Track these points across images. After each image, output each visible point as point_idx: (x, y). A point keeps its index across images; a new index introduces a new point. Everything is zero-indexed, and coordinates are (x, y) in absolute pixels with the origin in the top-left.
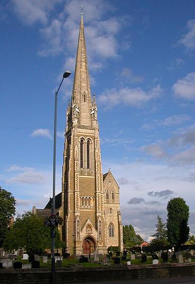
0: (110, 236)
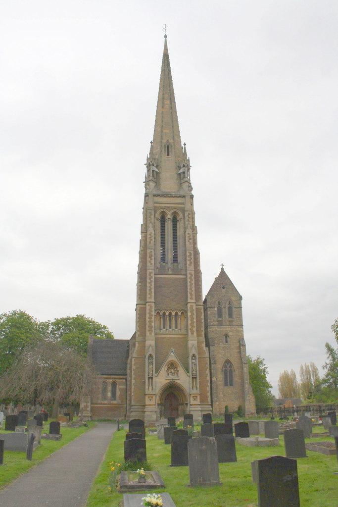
0: (226, 385)
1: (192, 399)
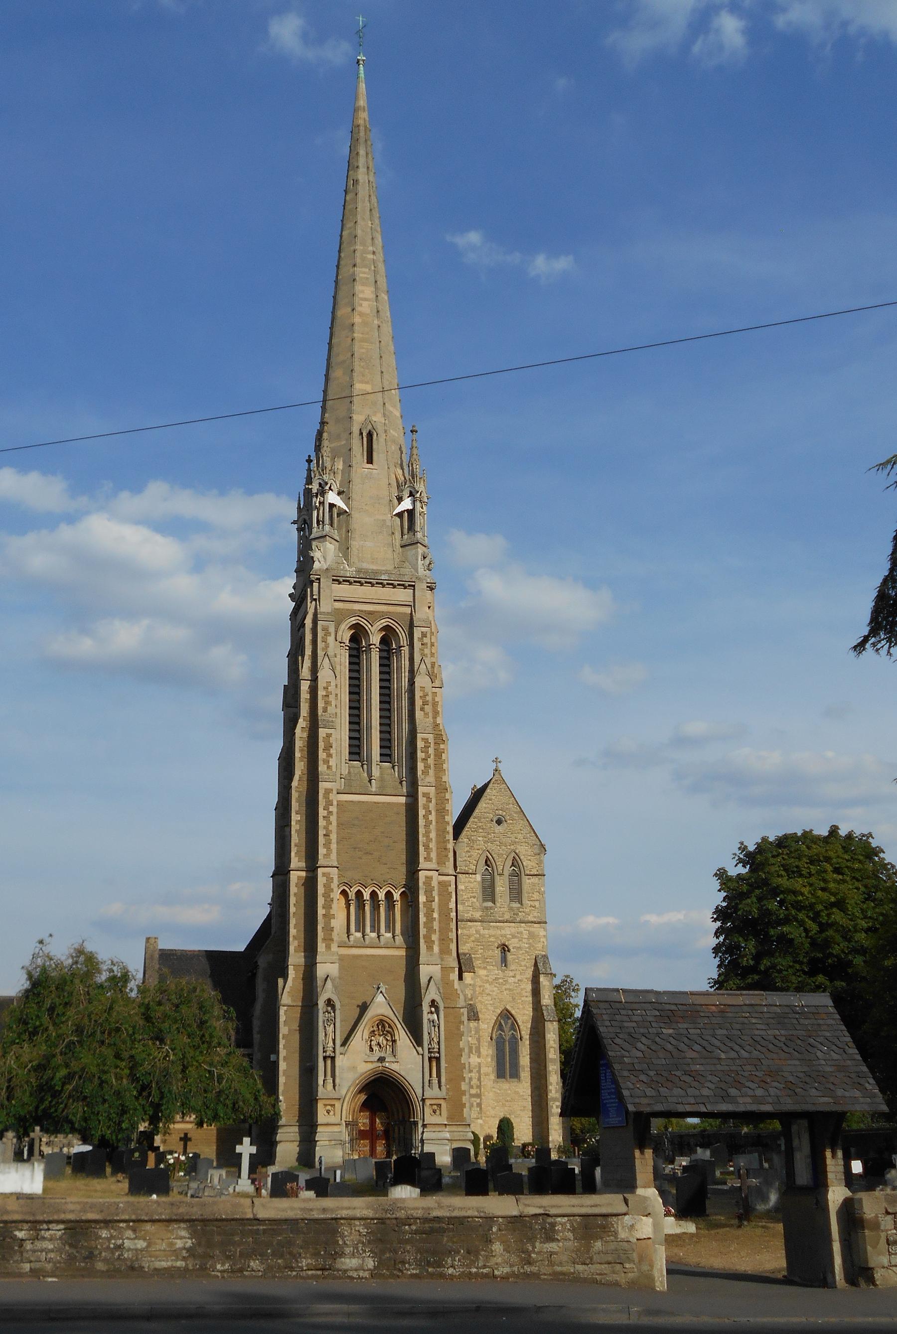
1: (428, 1110)
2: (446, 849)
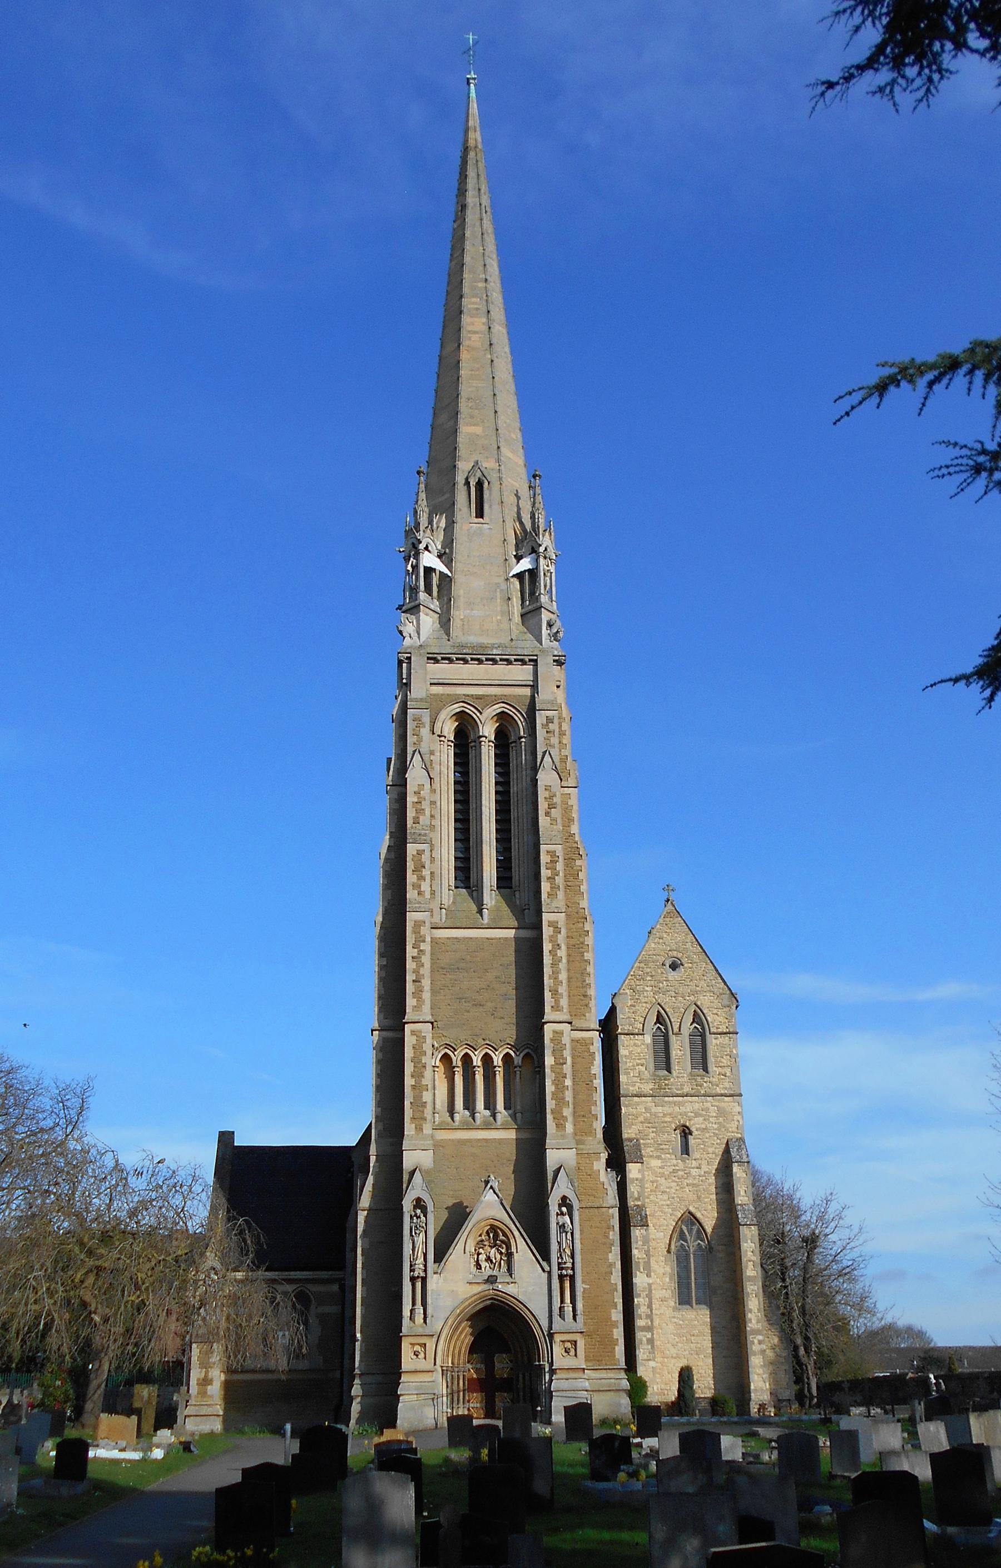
1: (558, 1350)
2: (585, 996)
